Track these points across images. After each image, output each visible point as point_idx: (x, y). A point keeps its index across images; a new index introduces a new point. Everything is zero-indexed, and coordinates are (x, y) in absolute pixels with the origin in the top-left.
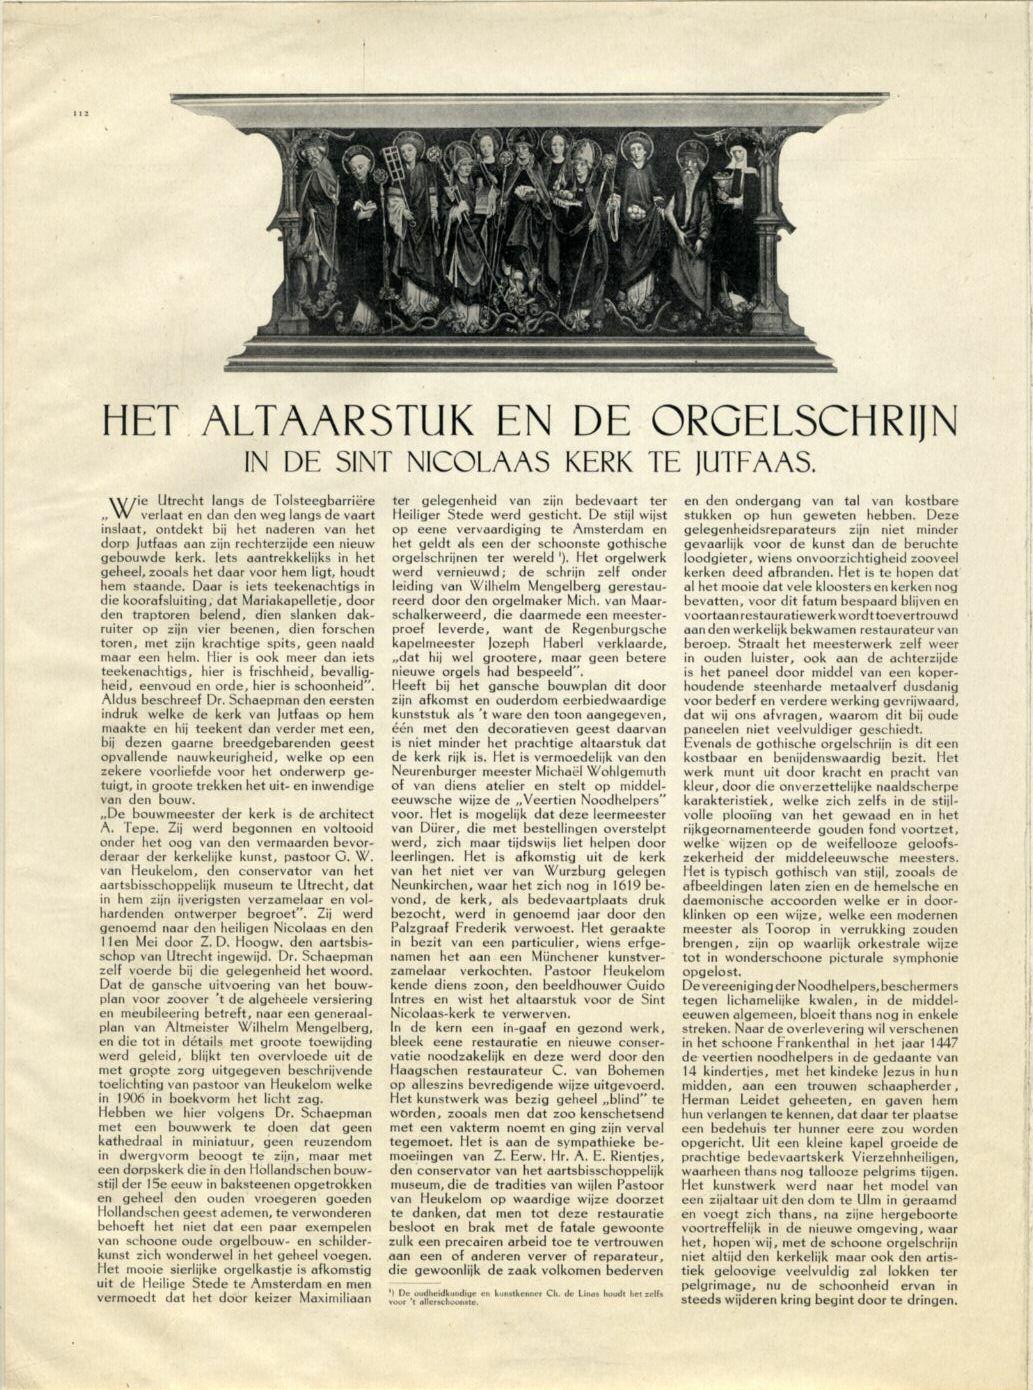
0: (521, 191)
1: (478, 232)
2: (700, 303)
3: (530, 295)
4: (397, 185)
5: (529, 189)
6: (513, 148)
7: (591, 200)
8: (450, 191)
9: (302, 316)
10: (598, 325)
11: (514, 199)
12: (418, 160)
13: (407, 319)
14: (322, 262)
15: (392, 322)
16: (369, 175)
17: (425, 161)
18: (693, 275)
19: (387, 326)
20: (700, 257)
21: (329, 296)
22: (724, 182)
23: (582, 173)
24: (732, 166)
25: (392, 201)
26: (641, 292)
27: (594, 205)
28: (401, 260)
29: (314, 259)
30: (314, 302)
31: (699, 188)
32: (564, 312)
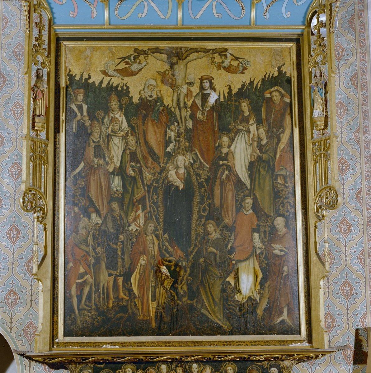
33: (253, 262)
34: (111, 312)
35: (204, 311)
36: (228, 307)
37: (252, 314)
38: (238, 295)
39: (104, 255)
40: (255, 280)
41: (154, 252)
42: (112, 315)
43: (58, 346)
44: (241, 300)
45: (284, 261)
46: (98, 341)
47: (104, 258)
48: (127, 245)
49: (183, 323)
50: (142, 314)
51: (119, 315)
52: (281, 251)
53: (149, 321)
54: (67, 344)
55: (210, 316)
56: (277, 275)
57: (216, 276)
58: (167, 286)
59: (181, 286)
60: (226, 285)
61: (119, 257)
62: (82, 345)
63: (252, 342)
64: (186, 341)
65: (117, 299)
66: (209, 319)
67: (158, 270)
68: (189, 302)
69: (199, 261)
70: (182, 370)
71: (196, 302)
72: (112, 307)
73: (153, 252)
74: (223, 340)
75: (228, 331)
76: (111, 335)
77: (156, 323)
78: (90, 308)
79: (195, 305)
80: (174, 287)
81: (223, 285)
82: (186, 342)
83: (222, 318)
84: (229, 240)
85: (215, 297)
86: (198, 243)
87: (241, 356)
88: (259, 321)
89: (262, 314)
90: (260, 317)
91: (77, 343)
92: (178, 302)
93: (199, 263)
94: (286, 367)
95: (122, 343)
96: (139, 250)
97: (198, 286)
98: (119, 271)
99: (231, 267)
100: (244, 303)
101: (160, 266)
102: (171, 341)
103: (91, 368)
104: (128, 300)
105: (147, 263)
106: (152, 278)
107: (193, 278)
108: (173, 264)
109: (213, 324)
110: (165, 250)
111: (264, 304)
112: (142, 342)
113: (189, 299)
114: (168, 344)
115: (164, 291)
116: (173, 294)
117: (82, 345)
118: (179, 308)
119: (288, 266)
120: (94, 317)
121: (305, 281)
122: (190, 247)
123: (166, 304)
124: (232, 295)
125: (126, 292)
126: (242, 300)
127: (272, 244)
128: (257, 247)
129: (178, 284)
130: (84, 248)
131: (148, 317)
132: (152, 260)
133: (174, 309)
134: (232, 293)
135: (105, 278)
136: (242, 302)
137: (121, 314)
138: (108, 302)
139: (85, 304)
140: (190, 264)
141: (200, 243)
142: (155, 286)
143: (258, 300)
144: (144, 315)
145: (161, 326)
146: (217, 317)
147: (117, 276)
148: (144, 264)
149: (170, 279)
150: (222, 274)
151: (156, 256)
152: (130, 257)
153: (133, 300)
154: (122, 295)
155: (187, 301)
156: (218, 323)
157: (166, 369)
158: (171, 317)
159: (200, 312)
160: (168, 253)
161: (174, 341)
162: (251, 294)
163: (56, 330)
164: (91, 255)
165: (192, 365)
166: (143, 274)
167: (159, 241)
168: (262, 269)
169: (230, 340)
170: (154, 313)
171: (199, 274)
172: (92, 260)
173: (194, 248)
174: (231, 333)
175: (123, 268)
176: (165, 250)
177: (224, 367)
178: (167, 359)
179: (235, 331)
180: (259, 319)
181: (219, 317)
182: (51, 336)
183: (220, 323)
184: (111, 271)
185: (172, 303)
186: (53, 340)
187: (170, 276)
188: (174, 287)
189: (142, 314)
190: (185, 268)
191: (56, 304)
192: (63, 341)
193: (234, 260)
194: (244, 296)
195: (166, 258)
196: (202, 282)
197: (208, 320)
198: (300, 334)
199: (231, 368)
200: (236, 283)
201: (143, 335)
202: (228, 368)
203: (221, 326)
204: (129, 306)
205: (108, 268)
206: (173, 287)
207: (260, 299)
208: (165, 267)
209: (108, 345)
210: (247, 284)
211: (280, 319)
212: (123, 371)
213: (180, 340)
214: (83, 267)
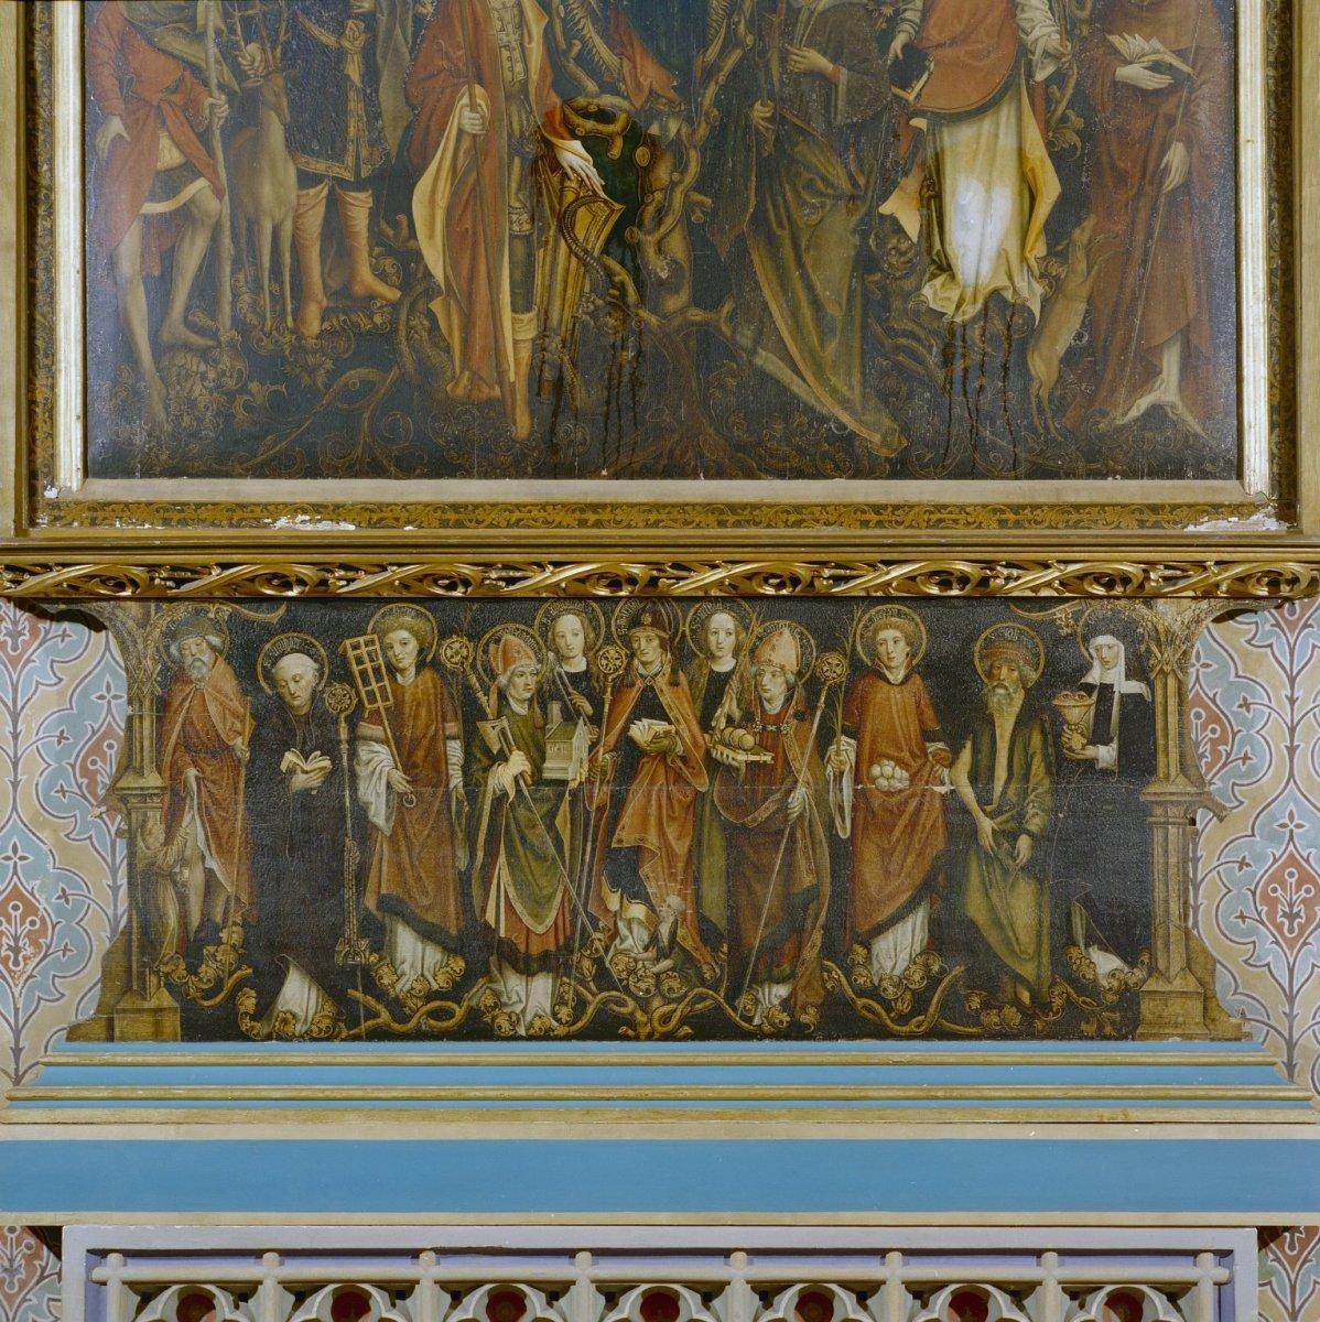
0: (643, 731)
1: (551, 815)
2: (1027, 971)
3: (662, 955)
4: (375, 718)
5: (660, 726)
6: (627, 642)
7: (794, 752)
8: (491, 732)
9: (166, 999)
10: (809, 1017)
11: (631, 757)
12: (420, 665)
13: (397, 1007)
15: (361, 1008)
16: (316, 696)
17: (436, 664)
18: (1016, 911)
19: (353, 1022)
21: (225, 956)
22: (1076, 710)
24: (1094, 677)
25: (363, 752)
26: (898, 950)
28: (382, 880)
30: (193, 970)
31: (1021, 722)
32: (732, 996)
33: (1013, 120)
34: (311, 360)
35: (767, 360)
36: (888, 342)
37: (1005, 378)
38: (938, 281)
39: (280, 82)
40: (1022, 210)
41: (527, 70)
42: (320, 379)
43: (57, 519)
44: (950, 310)
45: (1171, 121)
46: (253, 500)
47: (277, 95)
48: (390, 31)
49: (667, 418)
50: (467, 373)
51: (354, 376)
52: (1156, 67)
53: (497, 410)
54: (99, 511)
55: (797, 387)
56: (1135, 190)
57: (830, 191)
58: (587, 240)
59: (657, 236)
60: (877, 237)
61: (352, 95)
62: (177, 516)
63: (1003, 512)
64: (680, 500)
65: (345, 296)
66: (794, 396)
67: (547, 160)
68: (697, 315)
69: (747, 117)
70: (662, 640)
71: (731, 317)
72: (320, 336)
73: (519, 67)
74: (859, 499)
75: (888, 460)
76: (313, 472)
77: (532, 413)
78: (210, 343)
79: (726, 330)
80: (623, 243)
81: (864, 235)
82: (682, 507)
83: (856, 395)
84: (897, 12)
85: (825, 294)
86: (742, 27)
87: (945, 566)
88: (1041, 411)
89: (1055, 376)
90: (1044, 394)
91: (149, 504)
92: (644, 314)
93: (748, 126)
94: (1167, 632)
95: (367, 508)
96: (449, 59)
97: (741, 238)
98: (350, 161)
99: (904, 147)
100: (964, 326)
101: (555, 140)
102: (608, 500)
103: (216, 626)
104: (395, 306)
105: (492, 124)
106: (516, 199)
107: (716, 197)
108: (616, 128)
109: (811, 425)
110: (579, 59)
111: (1064, 332)
112: (465, 506)
113: (697, 301)
114: (592, 517)
115: (574, 259)
116: (617, 279)
117: (177, 516)
118: (647, 348)
119: (1189, 146)
120: (231, 383)
121: (1271, 217)
122: (704, 46)
123: (585, 326)
124: (908, 284)
125: (388, 264)
126: (958, 307)
127: (1111, 33)
128: (1039, 51)
129: (640, 225)
130: (178, 45)
131: (497, 389)
132: (514, 109)
133: (623, 348)
134: (907, 276)
135: (283, 192)
136: (958, 320)
137: (364, 372)
138: (298, 314)
139: (186, 322)
140: (703, 130)
141: (751, 24)
142: (527, 239)
143: (1036, 308)
144: (475, 378)
145: (560, 431)
146: (834, 391)
147: (342, 182)
148: (476, 130)
149: (605, 202)
150: (862, 181)
151: (532, 90)
152: (407, 97)
153: (421, 306)
154: (366, 278)
155: (683, 310)
156: (837, 421)
157: (581, 636)
158: (609, 388)
159: (750, 362)
160: (594, 70)
161: (622, 499)
162: (1002, 281)
163: (49, 443)
164: (214, 82)
165: (709, 617)
166: (472, 179)
167: (549, 13)
168: (1058, 157)
169: (895, 499)
170: (524, 369)
171: (747, 179)
172: (218, 107)
173: (722, 54)
174: (901, 468)
175: (372, 146)
176: (579, 59)
177: (866, 627)
178: (582, 579)
179: (919, 458)
180: (1039, 403)
181: (844, 390)
182: (24, 471)
183: (845, 418)
184: (312, 161)
185: (611, 321)
186: (33, 492)
187: (605, 188)
188: (623, 243)
189: (467, 373)
190: (678, 149)
191: (43, 315)
192: (80, 497)
193: (920, 113)
194: (969, 292)
195: (581, 101)
196: (760, 219)
197: (788, 404)
198: (1240, 476)
199: (898, 634)
200: (929, 224)
201: (467, 474)
202: (883, 635)
203: (853, 436)
204: (403, 333)
205: (296, 143)
206: (620, 241)
207: (1046, 303)
208: (577, 145)
209: (301, 517)
210: (983, 224)
211: (1143, 403)
212: (373, 642)
213: (651, 499)
214: (172, 139)
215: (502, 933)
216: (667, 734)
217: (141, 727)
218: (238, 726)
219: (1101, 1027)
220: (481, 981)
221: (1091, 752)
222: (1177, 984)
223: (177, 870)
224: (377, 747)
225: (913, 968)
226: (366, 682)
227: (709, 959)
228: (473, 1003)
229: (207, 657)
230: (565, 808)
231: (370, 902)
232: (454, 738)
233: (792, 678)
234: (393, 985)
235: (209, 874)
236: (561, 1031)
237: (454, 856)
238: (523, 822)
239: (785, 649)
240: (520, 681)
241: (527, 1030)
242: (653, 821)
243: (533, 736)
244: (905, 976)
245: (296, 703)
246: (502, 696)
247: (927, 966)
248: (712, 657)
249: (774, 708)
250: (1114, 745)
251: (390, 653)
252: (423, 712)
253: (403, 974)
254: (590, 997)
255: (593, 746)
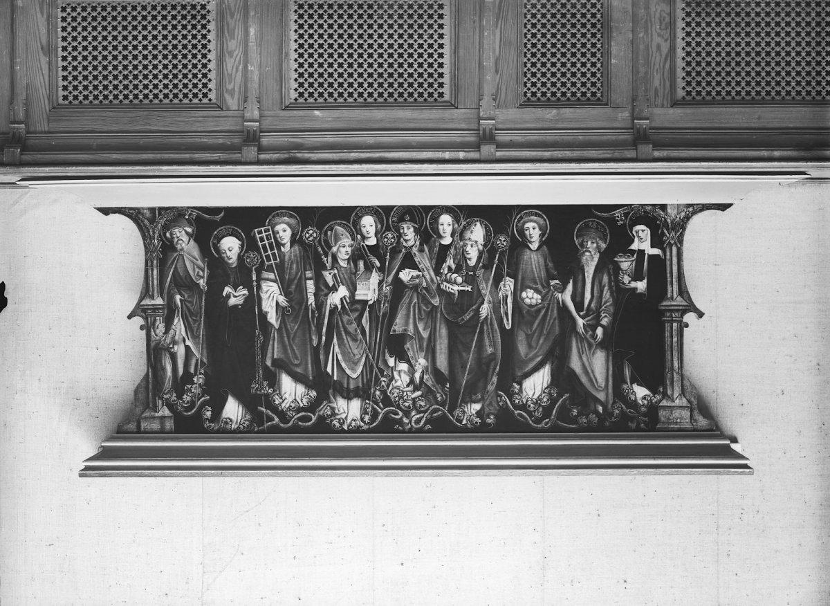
0: (405, 275)
2: (601, 396)
3: (416, 389)
4: (270, 269)
5: (415, 273)
6: (397, 229)
7: (482, 285)
8: (329, 277)
9: (166, 412)
10: (491, 420)
13: (282, 415)
14: (187, 348)
15: (265, 418)
16: (240, 257)
20: (603, 345)
21: (195, 389)
22: (626, 264)
23: (473, 254)
24: (635, 246)
26: (536, 385)
27: (486, 289)
28: (275, 350)
29: (180, 350)
30: (180, 397)
31: (598, 270)
32: (451, 411)
157: (374, 227)
165: (439, 216)
177: (519, 221)
199: (535, 225)
202: (527, 225)
215: (335, 378)
216: (418, 276)
217: (152, 274)
218: (201, 273)
219: (638, 424)
220: (325, 403)
221: (633, 284)
222: (677, 402)
223: (171, 346)
224: (271, 284)
225: (543, 395)
226: (266, 251)
227: (440, 391)
228: (321, 413)
229: (185, 238)
230: (366, 314)
231: (269, 363)
232: (310, 279)
233: (481, 248)
234: (280, 404)
235: (187, 348)
236: (366, 427)
237: (311, 340)
238: (345, 322)
239: (477, 233)
240: (343, 250)
241: (348, 427)
242: (411, 321)
243: (350, 278)
244: (539, 399)
245: (230, 261)
246: (335, 258)
247: (550, 394)
248: (440, 237)
249: (472, 263)
250: (645, 281)
251: (278, 236)
252: (295, 266)
253: (286, 399)
254: (380, 410)
255: (380, 283)
